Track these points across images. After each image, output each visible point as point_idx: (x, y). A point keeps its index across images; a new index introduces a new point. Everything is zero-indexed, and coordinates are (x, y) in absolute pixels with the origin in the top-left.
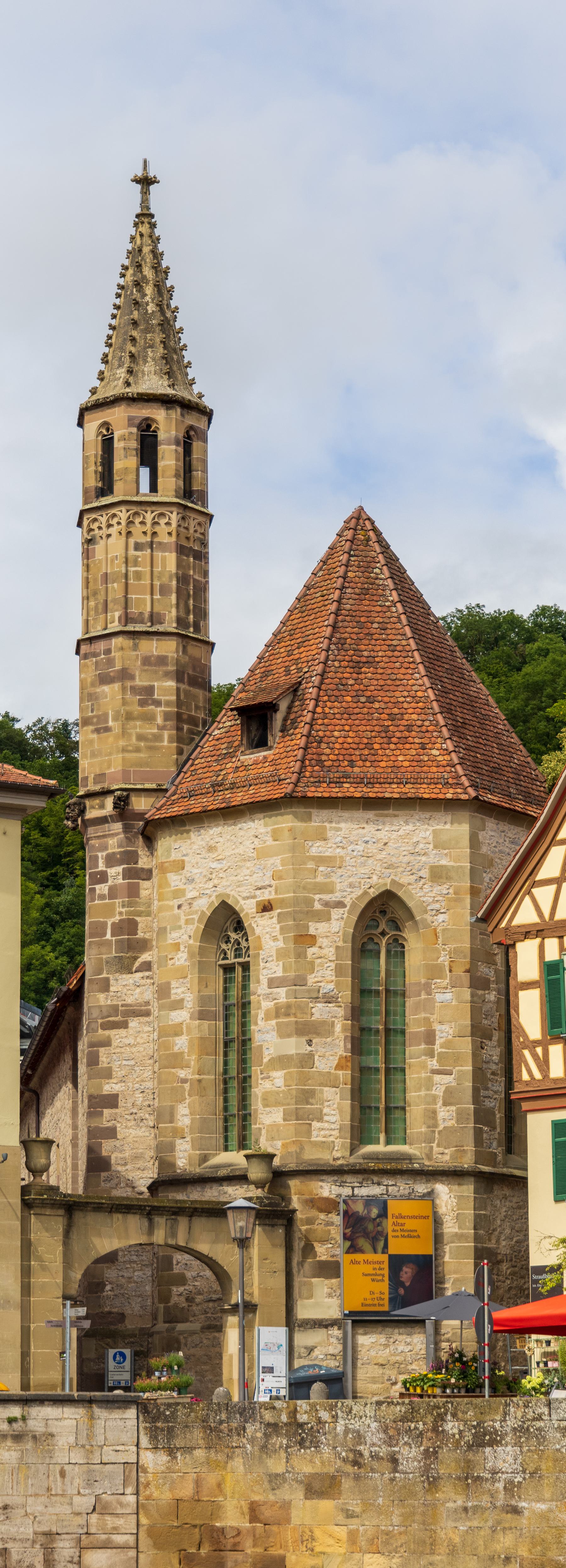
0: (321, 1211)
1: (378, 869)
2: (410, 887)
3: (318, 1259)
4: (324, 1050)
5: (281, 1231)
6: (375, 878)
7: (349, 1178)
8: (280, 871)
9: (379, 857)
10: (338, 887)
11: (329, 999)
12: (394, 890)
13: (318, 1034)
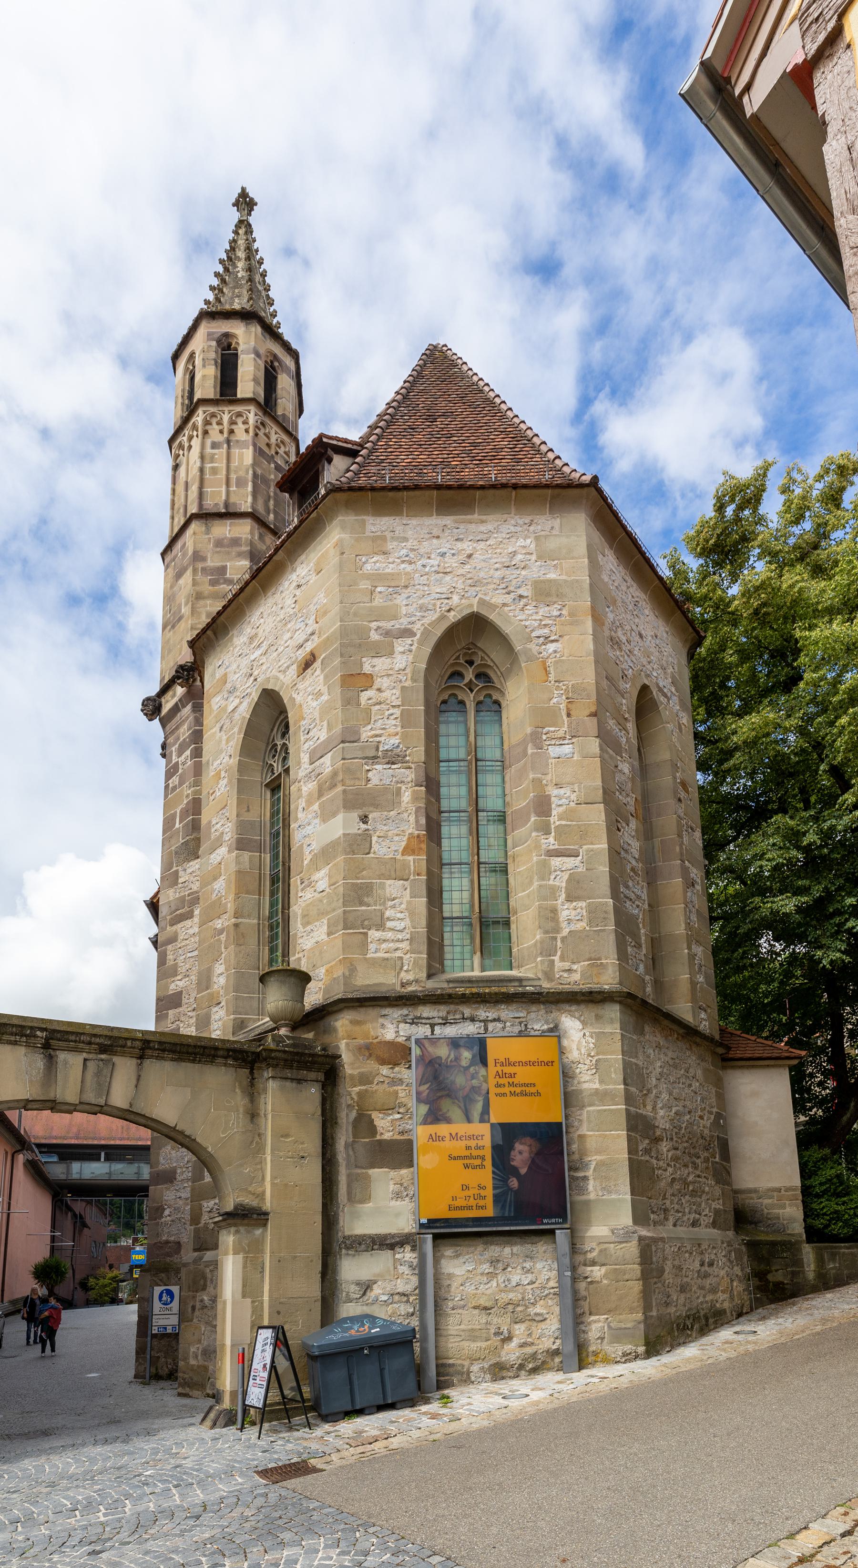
0: (383, 1062)
1: (460, 585)
2: (506, 609)
3: (378, 1137)
4: (385, 828)
5: (314, 1092)
6: (456, 599)
7: (426, 1011)
8: (325, 604)
9: (461, 571)
10: (404, 610)
11: (393, 758)
12: (484, 612)
13: (377, 806)
